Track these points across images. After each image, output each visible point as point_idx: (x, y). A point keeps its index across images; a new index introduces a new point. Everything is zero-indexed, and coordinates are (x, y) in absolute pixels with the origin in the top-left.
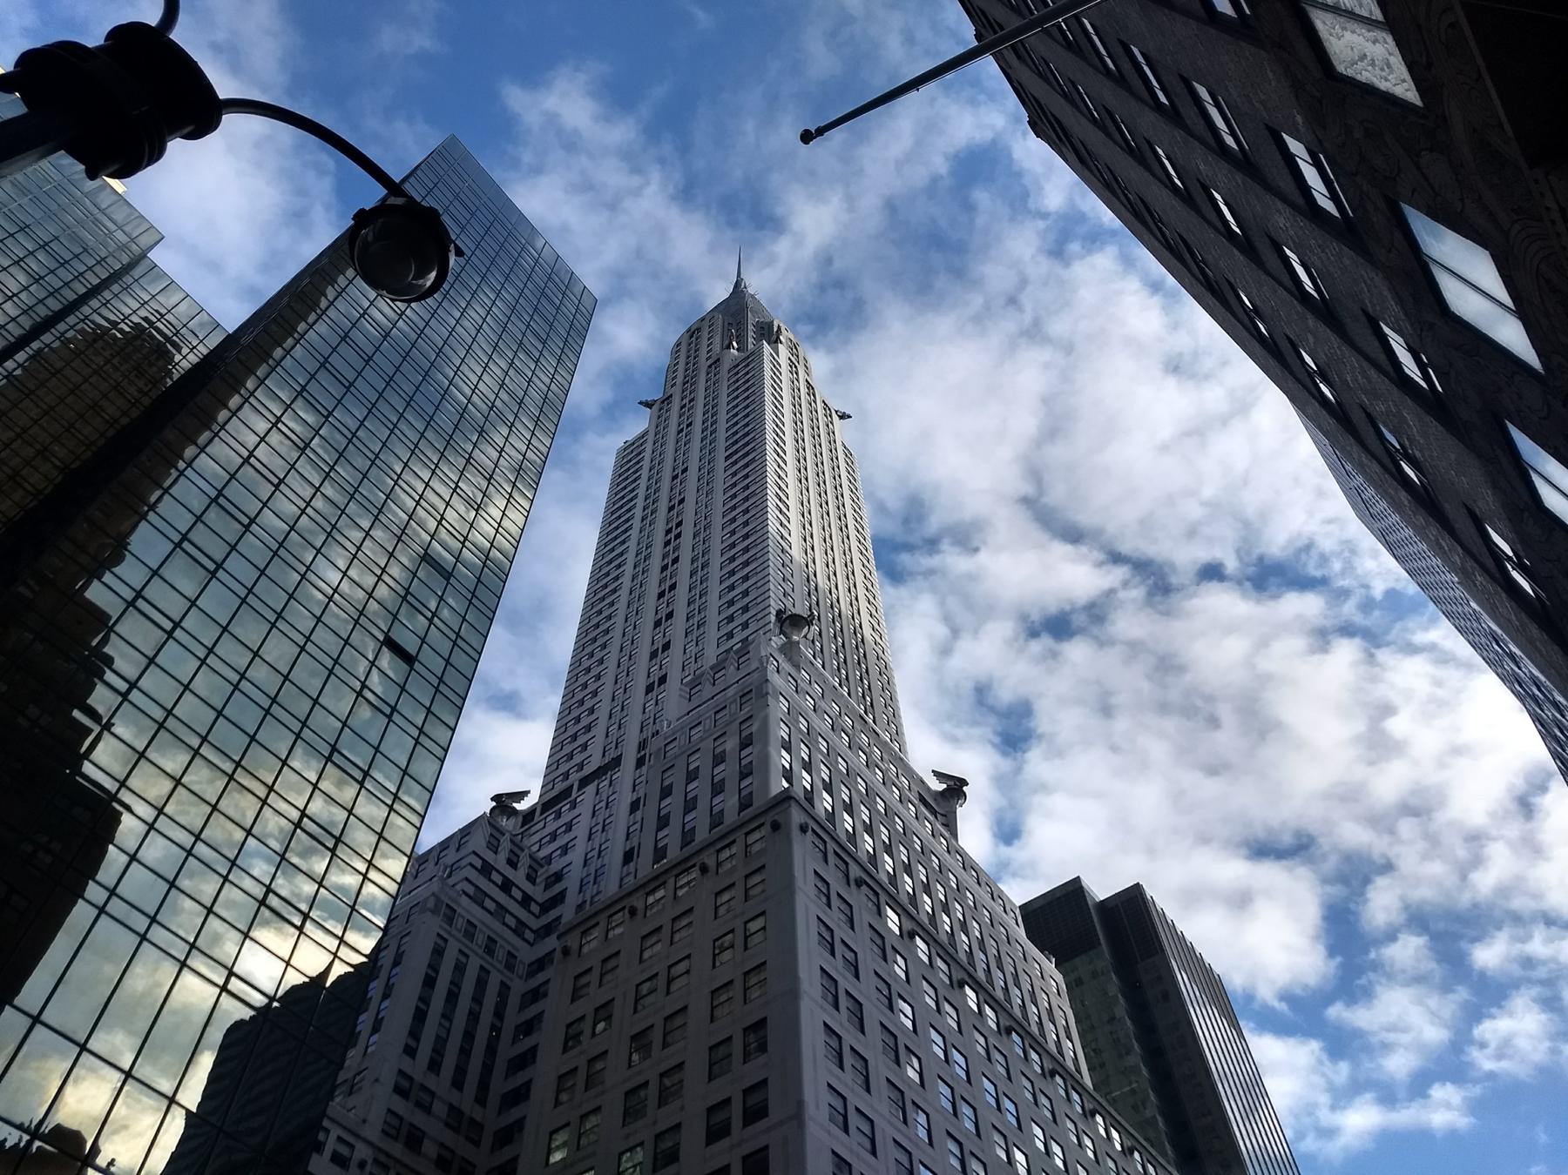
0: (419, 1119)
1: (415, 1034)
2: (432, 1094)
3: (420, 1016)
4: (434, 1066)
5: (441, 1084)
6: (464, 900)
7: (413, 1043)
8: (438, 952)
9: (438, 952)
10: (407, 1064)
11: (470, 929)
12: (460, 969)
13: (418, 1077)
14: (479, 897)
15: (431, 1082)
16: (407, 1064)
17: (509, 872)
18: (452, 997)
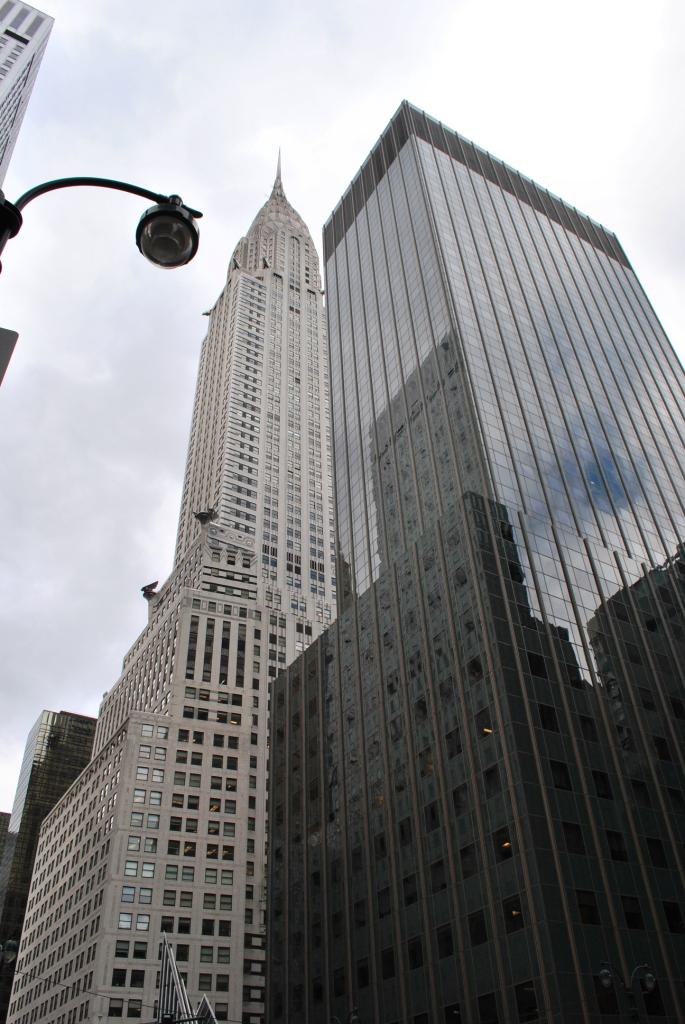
0: (204, 705)
1: (191, 667)
2: (209, 691)
3: (191, 656)
4: (206, 679)
5: (214, 684)
6: (206, 593)
7: (190, 672)
8: (195, 624)
9: (195, 624)
10: (189, 683)
11: (212, 605)
12: (211, 627)
13: (198, 687)
14: (213, 588)
15: (206, 685)
16: (189, 683)
17: (231, 568)
18: (209, 641)
